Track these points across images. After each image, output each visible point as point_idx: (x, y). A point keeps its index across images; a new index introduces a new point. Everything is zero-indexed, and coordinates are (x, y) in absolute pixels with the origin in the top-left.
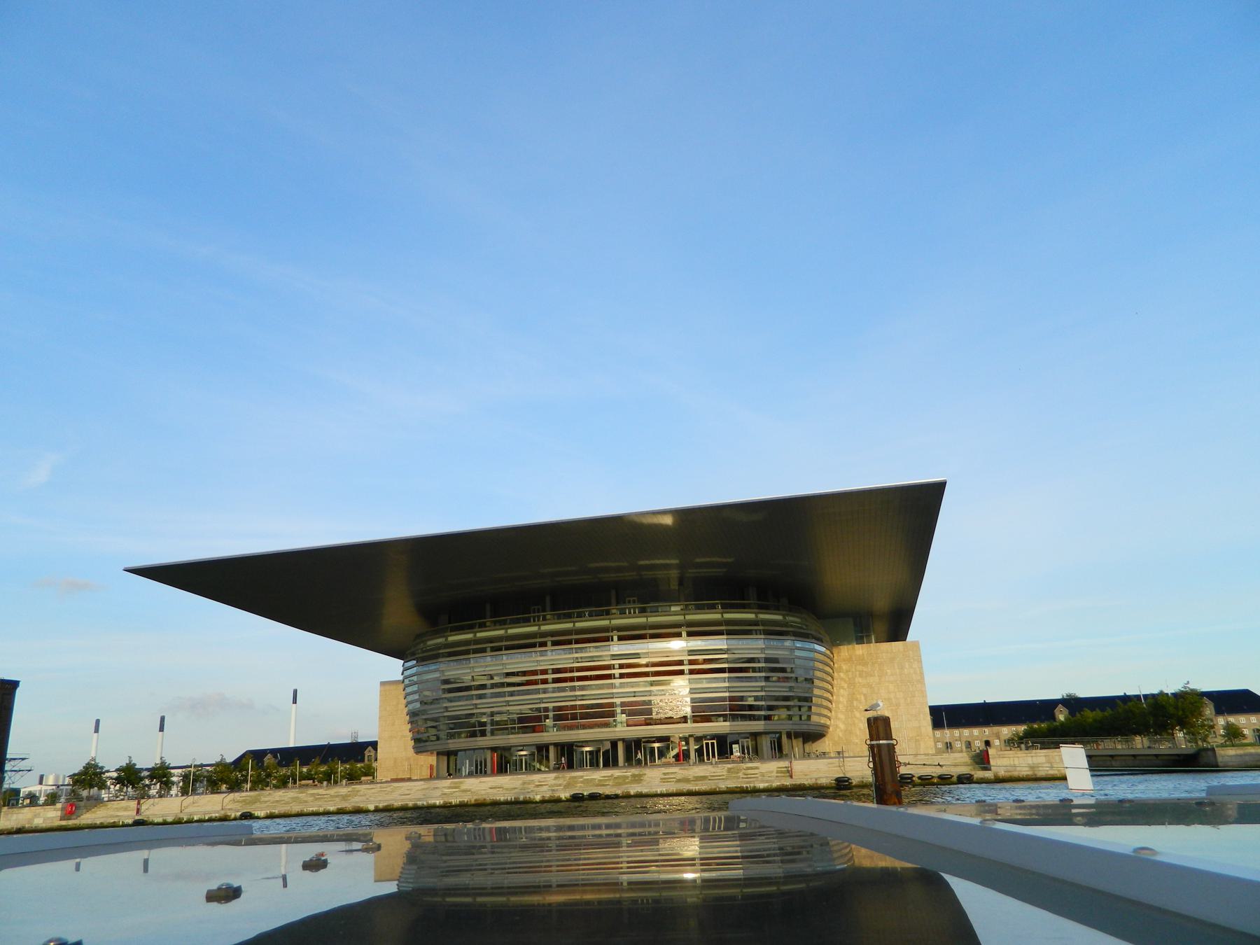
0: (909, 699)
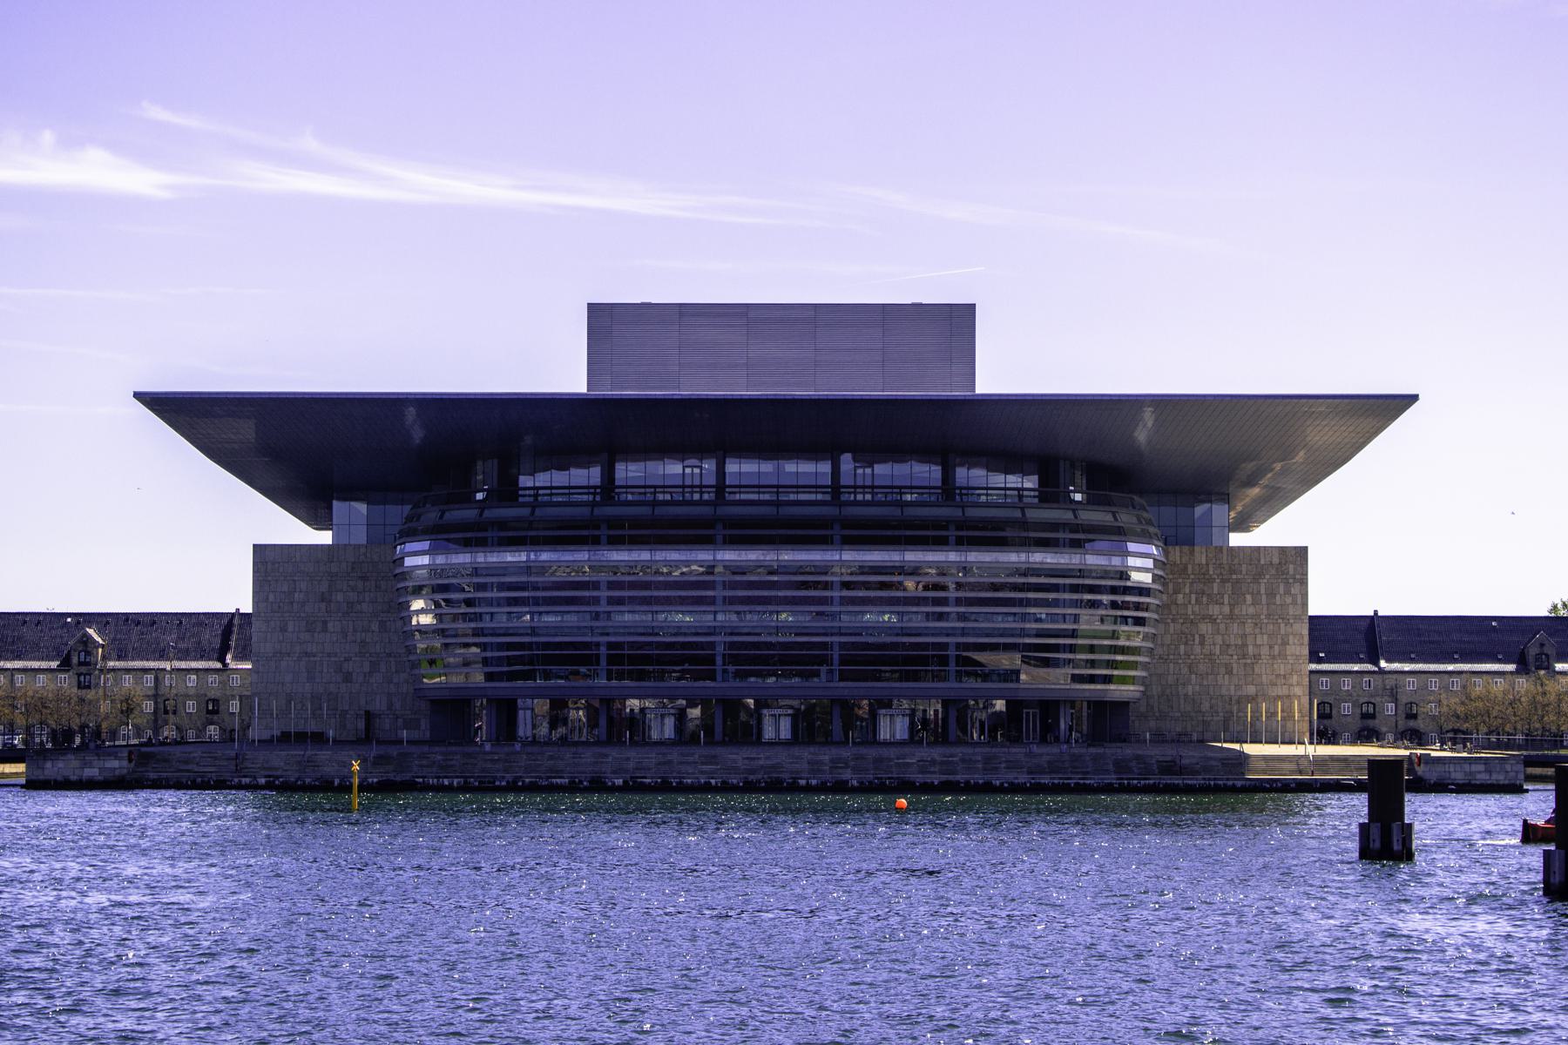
0: (1276, 647)
